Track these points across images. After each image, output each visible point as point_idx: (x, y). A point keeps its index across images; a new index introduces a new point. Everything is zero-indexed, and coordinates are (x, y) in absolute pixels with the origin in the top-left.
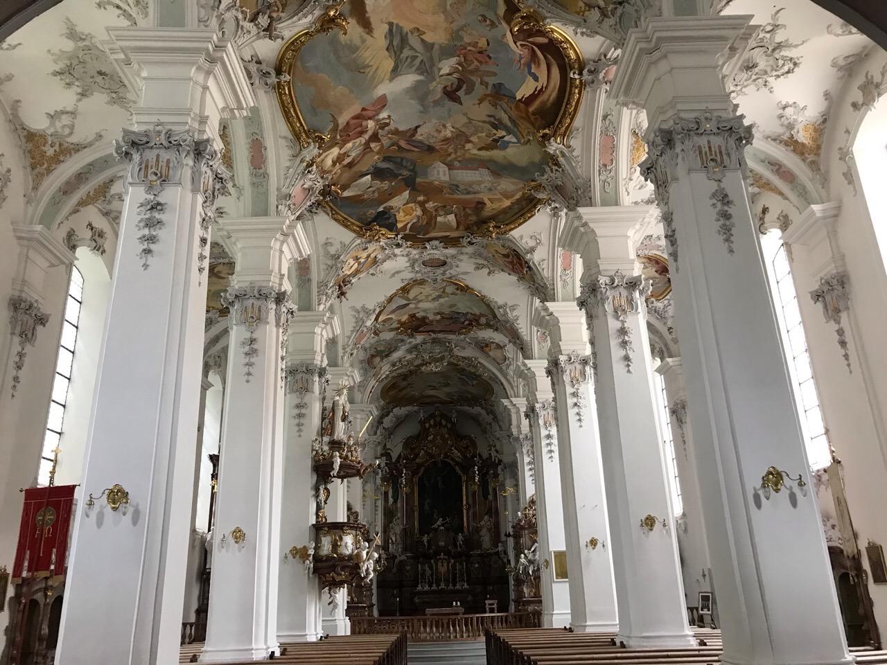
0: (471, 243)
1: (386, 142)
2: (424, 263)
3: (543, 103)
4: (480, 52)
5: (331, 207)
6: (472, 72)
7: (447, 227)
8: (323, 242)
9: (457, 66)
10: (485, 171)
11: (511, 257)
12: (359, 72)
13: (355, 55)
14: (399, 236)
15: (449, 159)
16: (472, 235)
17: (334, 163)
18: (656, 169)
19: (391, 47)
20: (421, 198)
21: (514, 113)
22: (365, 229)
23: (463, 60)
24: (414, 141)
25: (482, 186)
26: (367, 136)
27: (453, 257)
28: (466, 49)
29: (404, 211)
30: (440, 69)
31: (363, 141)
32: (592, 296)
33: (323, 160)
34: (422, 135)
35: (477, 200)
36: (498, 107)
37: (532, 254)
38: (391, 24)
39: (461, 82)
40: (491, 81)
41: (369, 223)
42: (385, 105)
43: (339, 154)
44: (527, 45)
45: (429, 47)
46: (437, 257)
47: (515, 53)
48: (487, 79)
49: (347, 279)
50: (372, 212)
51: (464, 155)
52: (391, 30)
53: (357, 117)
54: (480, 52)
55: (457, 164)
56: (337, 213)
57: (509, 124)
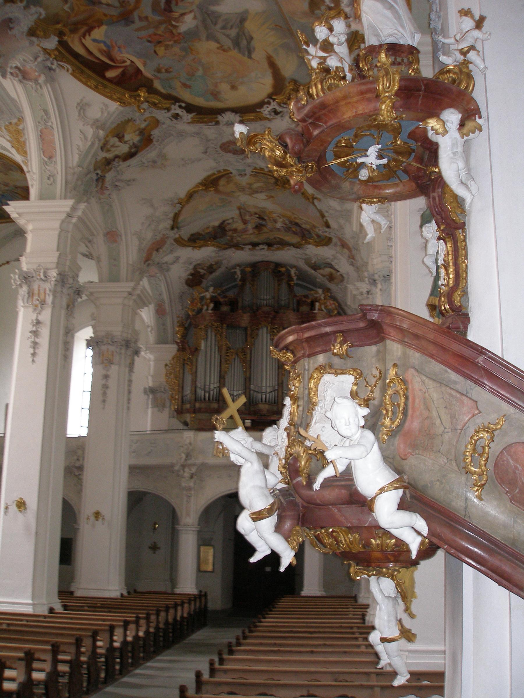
6: (161, 23)
9: (177, 24)
12: (281, 27)
23: (174, 31)
28: (175, 42)
30: (195, 18)
38: (250, 57)
40: (138, 24)
44: (121, 63)
45: (211, 37)
48: (144, 23)
54: (159, 42)
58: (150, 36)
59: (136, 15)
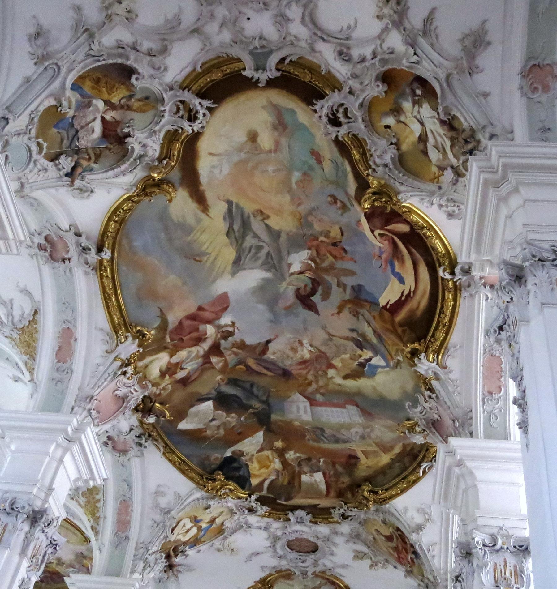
0: (344, 517)
1: (231, 358)
2: (290, 545)
3: (412, 312)
4: (334, 245)
5: (165, 443)
7: (313, 491)
8: (153, 490)
9: (310, 262)
10: (353, 409)
11: (395, 540)
12: (195, 260)
13: (189, 238)
14: (254, 497)
15: (310, 389)
16: (346, 504)
17: (163, 374)
18: (509, 326)
19: (231, 231)
20: (279, 444)
21: (377, 325)
22: (207, 478)
23: (315, 253)
24: (266, 361)
25: (353, 430)
26: (206, 346)
27: (327, 539)
28: (317, 239)
29: (259, 462)
30: (290, 265)
31: (202, 353)
32: (465, 563)
33: (146, 367)
34: (274, 353)
35: (349, 452)
36: (361, 317)
37: (418, 534)
38: (230, 203)
39: (316, 283)
40: (350, 281)
41: (212, 472)
42: (227, 308)
43: (169, 363)
45: (275, 235)
46: (305, 536)
47: (373, 245)
48: (344, 279)
49: (181, 548)
50: (217, 456)
51: (327, 385)
52: (230, 211)
53: (192, 317)
54: (334, 245)
55: (319, 397)
56: (173, 452)
57: (374, 340)
58: (342, 258)
59: (347, 297)
